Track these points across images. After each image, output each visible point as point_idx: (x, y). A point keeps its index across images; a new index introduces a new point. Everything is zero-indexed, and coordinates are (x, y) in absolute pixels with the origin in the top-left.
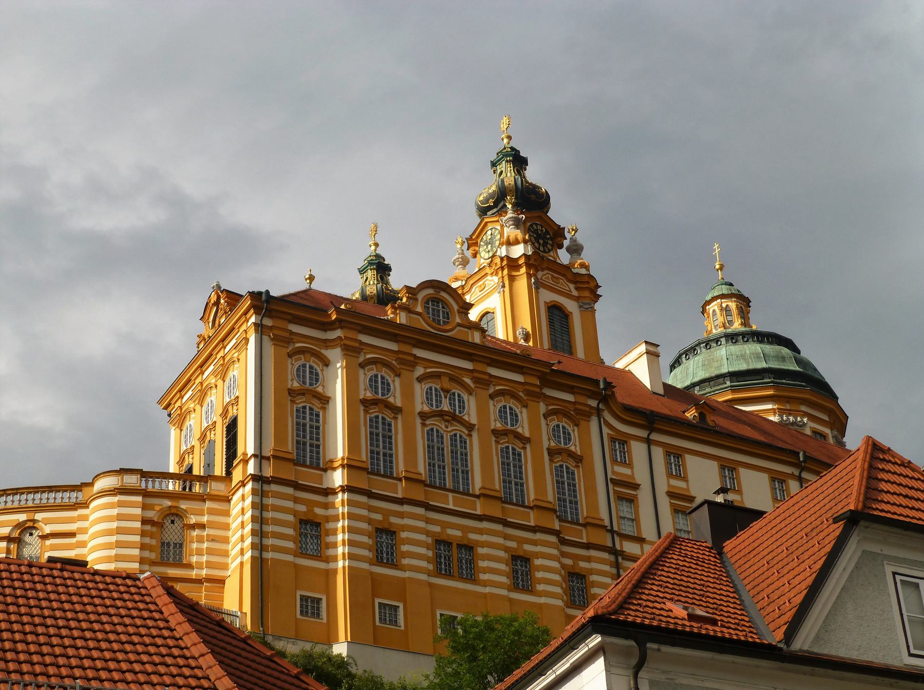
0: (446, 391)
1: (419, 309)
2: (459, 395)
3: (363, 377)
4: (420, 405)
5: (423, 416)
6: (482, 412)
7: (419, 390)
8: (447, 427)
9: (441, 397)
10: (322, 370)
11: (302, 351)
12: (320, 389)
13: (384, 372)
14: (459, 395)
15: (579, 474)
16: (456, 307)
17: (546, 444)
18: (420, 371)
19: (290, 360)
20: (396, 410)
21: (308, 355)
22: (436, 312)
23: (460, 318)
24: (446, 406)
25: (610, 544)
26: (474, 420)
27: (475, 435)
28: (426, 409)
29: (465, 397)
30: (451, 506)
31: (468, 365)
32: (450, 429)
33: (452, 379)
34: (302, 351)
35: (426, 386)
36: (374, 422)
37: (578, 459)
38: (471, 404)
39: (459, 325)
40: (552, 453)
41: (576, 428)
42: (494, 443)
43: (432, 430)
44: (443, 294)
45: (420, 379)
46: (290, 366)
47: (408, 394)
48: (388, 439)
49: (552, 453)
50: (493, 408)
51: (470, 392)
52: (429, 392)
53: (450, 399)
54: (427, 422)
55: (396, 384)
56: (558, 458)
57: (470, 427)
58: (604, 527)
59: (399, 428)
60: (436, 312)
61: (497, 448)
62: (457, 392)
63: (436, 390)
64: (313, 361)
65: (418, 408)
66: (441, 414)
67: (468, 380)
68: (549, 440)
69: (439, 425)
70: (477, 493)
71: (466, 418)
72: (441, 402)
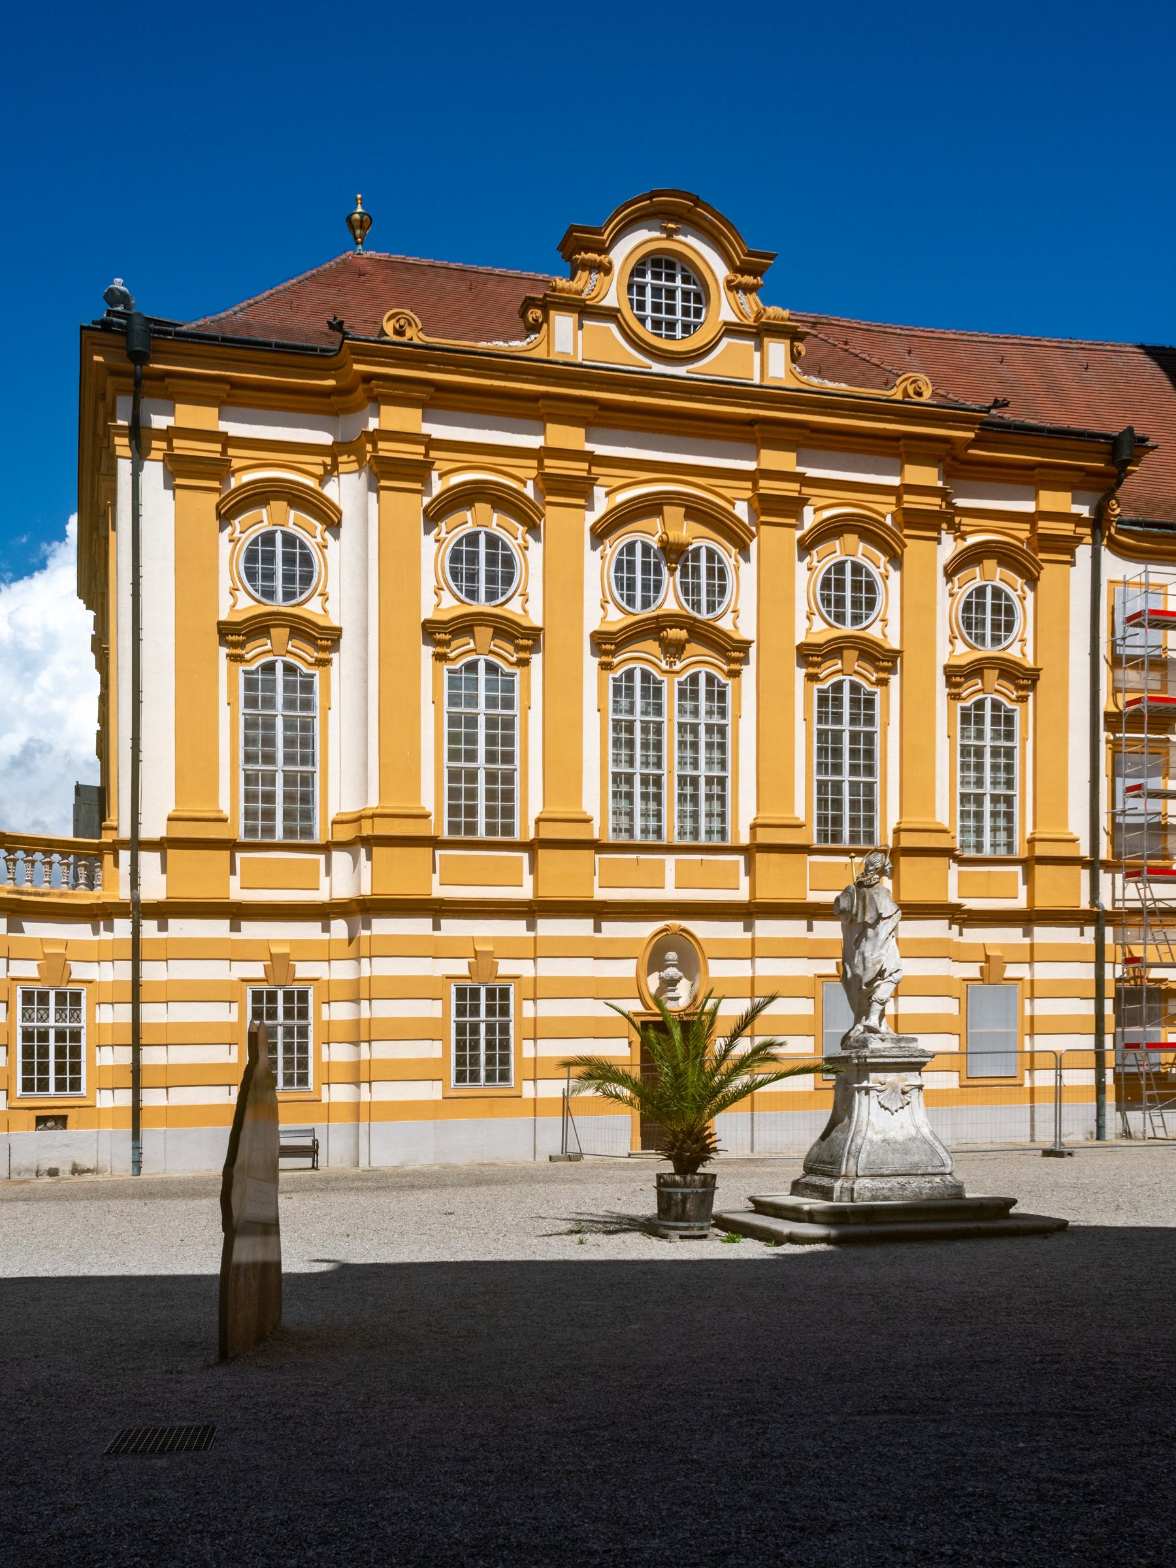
0: (674, 553)
2: (711, 554)
8: (671, 664)
9: (658, 572)
11: (260, 495)
13: (495, 522)
14: (711, 554)
15: (1024, 716)
21: (279, 506)
24: (670, 601)
26: (747, 630)
27: (749, 673)
28: (616, 619)
29: (728, 555)
30: (670, 893)
32: (679, 666)
33: (697, 511)
34: (260, 495)
35: (614, 546)
43: (629, 675)
46: (225, 548)
49: (956, 676)
52: (624, 565)
53: (684, 575)
56: (971, 691)
63: (646, 548)
64: (294, 521)
66: (653, 629)
70: (745, 839)
71: (725, 624)
72: (657, 588)
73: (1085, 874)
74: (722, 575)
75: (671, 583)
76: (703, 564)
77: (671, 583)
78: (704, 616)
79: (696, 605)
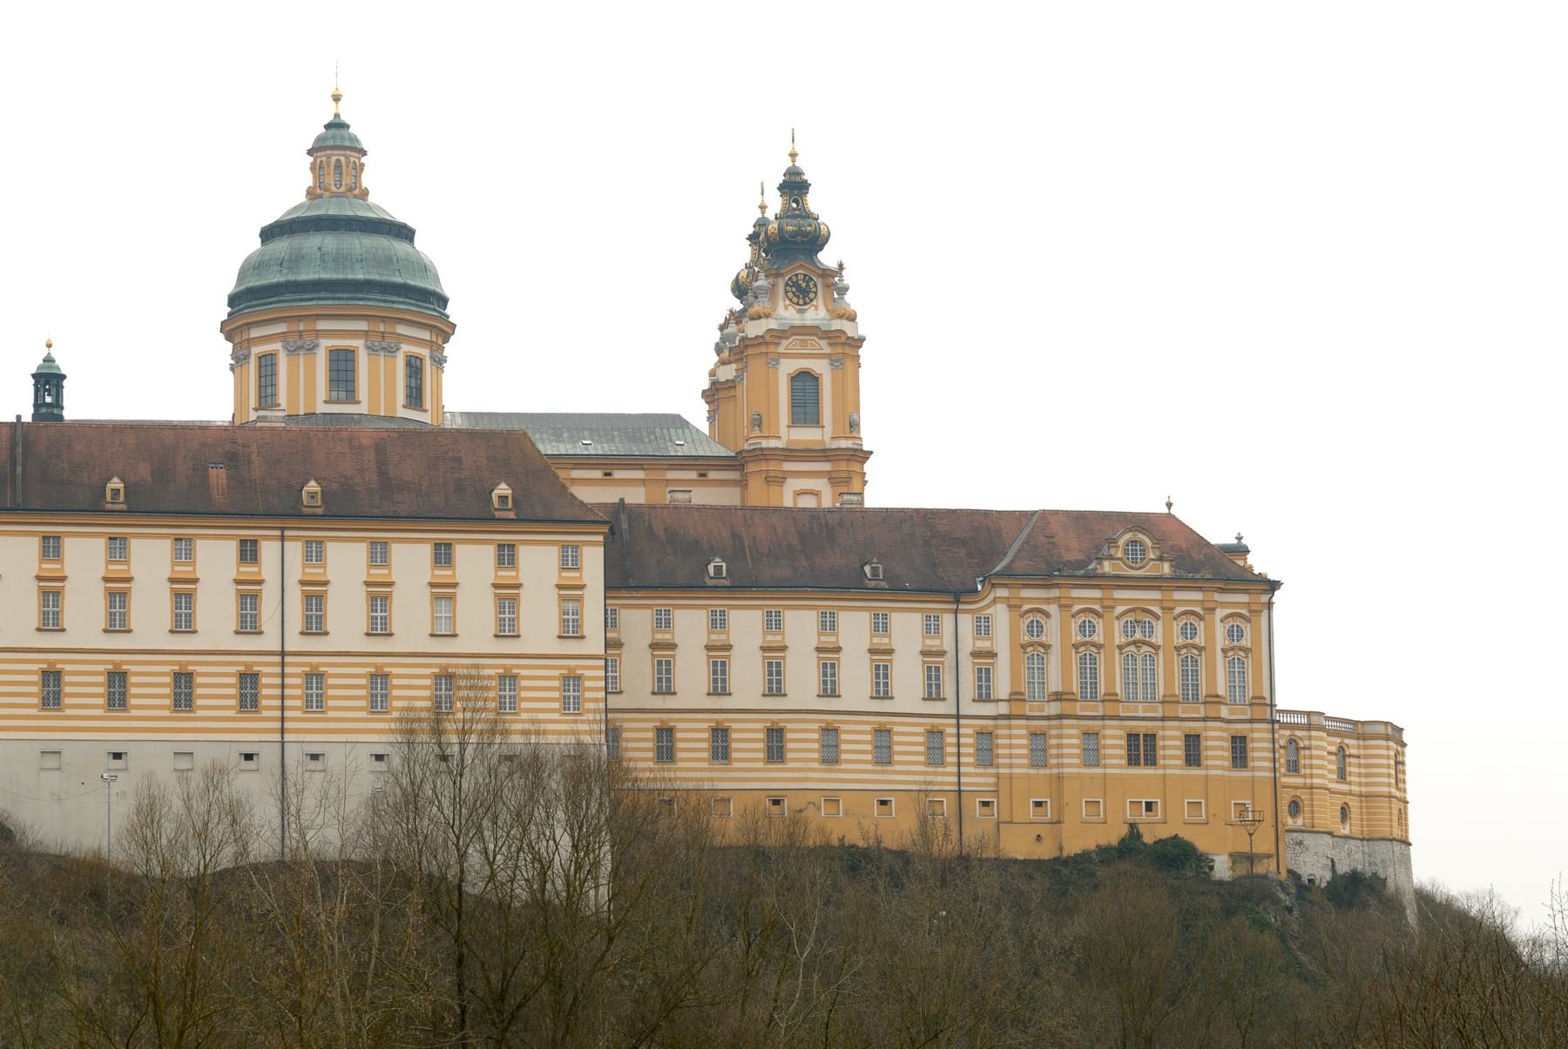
1: (1119, 555)
3: (1074, 625)
4: (1119, 639)
5: (1120, 648)
6: (1167, 635)
7: (1118, 626)
9: (1134, 627)
10: (1046, 623)
12: (1044, 638)
14: (1149, 622)
16: (1149, 543)
17: (1219, 645)
18: (1120, 609)
19: (1022, 619)
20: (1098, 646)
22: (1134, 552)
23: (1155, 555)
24: (1138, 636)
25: (1268, 717)
26: (1160, 642)
27: (1161, 652)
30: (1141, 714)
31: (1156, 595)
36: (1083, 659)
37: (1246, 650)
38: (1159, 627)
39: (1153, 560)
40: (1224, 651)
41: (1248, 625)
42: (1176, 657)
44: (1140, 536)
45: (1117, 618)
47: (1109, 633)
48: (1094, 671)
50: (1176, 627)
51: (1157, 618)
52: (1126, 626)
54: (1124, 651)
55: (1100, 625)
57: (1156, 648)
58: (1267, 705)
59: (1101, 659)
60: (1134, 552)
61: (1178, 659)
62: (1147, 620)
63: (1131, 622)
64: (1039, 617)
65: (1117, 643)
66: (1134, 643)
67: (1156, 609)
68: (1224, 640)
69: (1132, 648)
70: (1161, 700)
71: (1154, 641)
72: (1135, 631)
73: (1269, 708)
74: (1152, 627)
75: (1138, 630)
76: (1147, 625)
77: (1138, 630)
78: (1147, 639)
79: (1145, 637)
